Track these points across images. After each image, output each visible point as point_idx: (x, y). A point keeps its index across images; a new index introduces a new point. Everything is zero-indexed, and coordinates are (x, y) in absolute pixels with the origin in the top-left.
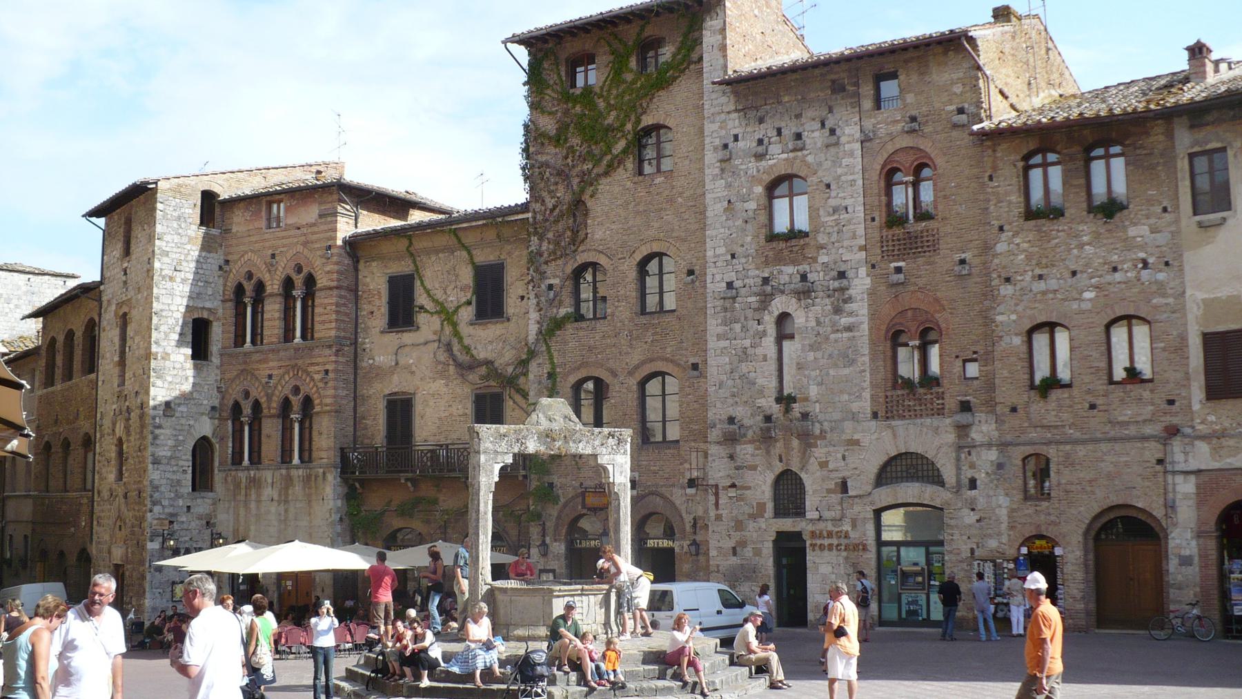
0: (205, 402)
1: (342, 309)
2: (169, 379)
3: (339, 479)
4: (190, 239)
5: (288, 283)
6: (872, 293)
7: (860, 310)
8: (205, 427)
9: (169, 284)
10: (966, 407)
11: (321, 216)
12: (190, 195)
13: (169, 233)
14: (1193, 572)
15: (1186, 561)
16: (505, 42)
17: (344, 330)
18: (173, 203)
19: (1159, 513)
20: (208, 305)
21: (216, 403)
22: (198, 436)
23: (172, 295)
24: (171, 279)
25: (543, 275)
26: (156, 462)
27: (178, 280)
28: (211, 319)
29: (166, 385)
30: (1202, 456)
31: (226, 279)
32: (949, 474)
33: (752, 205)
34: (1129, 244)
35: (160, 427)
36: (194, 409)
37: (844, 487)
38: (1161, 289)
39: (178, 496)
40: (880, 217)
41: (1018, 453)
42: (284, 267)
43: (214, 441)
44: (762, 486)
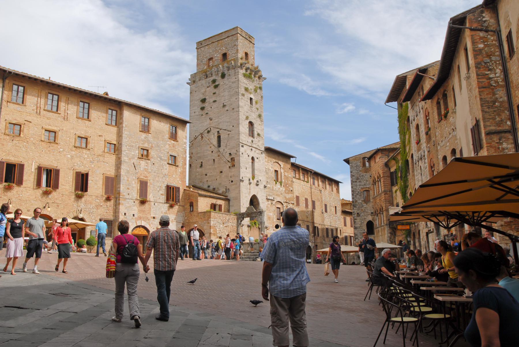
0: (369, 212)
1: (386, 182)
2: (358, 207)
3: (388, 228)
4: (360, 171)
5: (378, 177)
7: (426, 161)
8: (370, 218)
9: (355, 183)
11: (380, 158)
12: (359, 159)
13: (354, 170)
16: (385, 104)
17: (387, 188)
18: (354, 163)
20: (368, 186)
21: (373, 211)
22: (368, 220)
23: (356, 186)
24: (356, 182)
27: (358, 182)
28: (369, 190)
29: (357, 209)
35: (356, 219)
36: (366, 214)
42: (377, 174)
43: (373, 221)
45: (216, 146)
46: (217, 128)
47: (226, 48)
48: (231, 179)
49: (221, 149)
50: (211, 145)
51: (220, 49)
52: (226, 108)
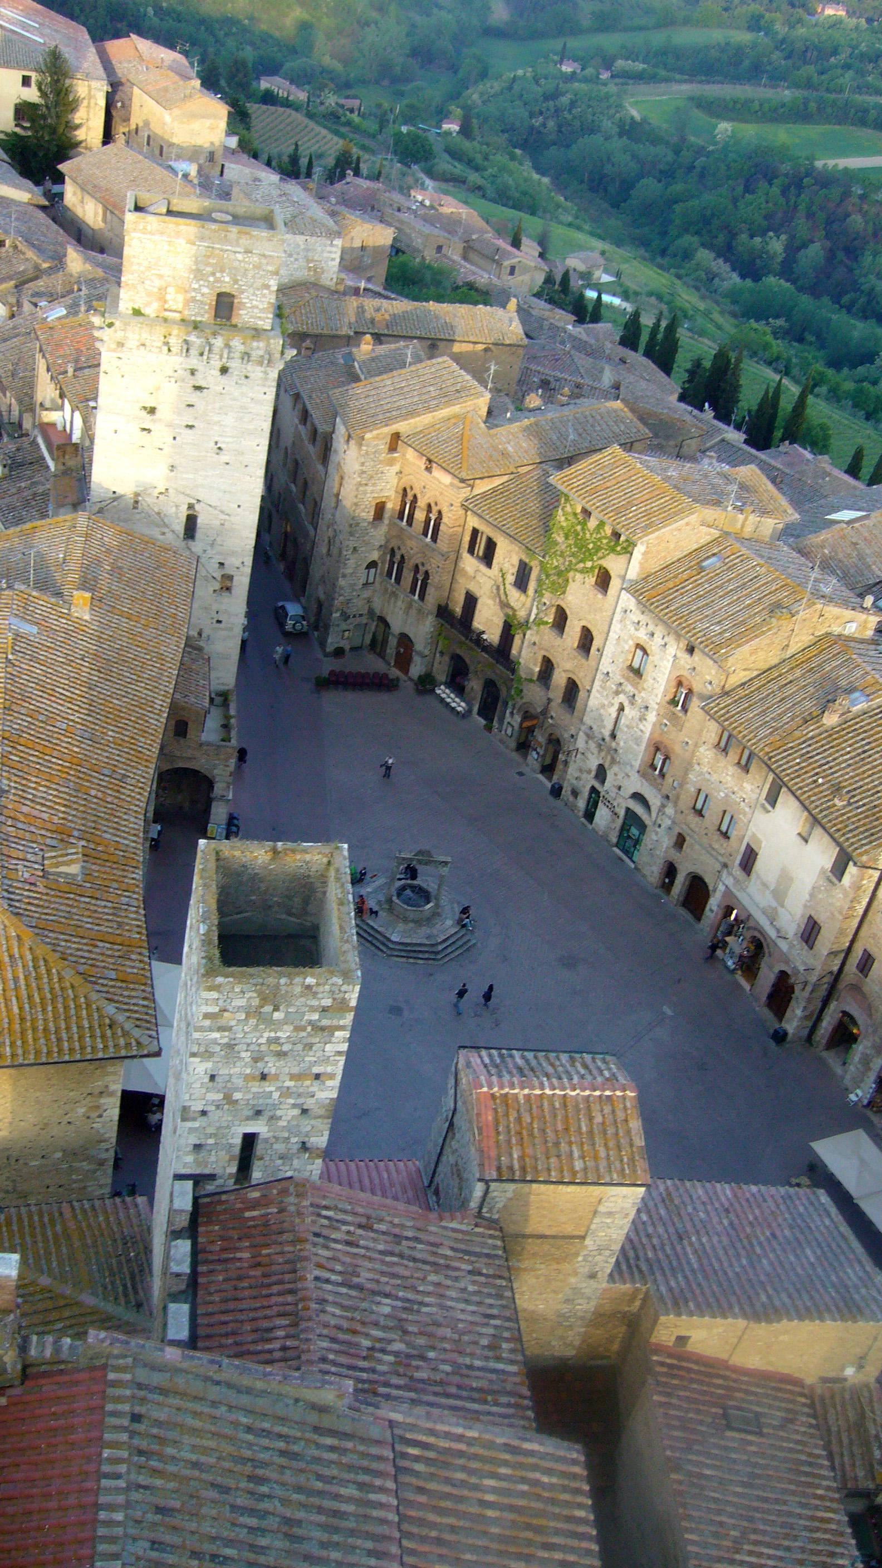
6: (654, 725)
8: (375, 556)
10: (668, 797)
14: (712, 915)
15: (711, 911)
19: (711, 888)
25: (542, 596)
26: (344, 576)
30: (729, 881)
31: (400, 479)
32: (654, 814)
33: (627, 647)
34: (742, 788)
37: (619, 788)
38: (745, 814)
39: (353, 590)
40: (669, 696)
41: (677, 830)
44: (593, 763)
45: (182, 536)
46: (188, 495)
47: (236, 282)
48: (216, 617)
49: (197, 546)
50: (166, 530)
51: (213, 274)
52: (224, 458)
